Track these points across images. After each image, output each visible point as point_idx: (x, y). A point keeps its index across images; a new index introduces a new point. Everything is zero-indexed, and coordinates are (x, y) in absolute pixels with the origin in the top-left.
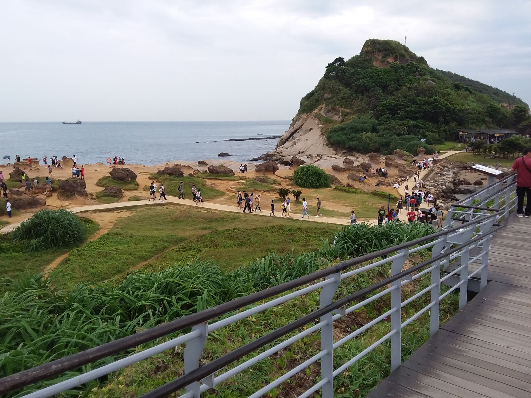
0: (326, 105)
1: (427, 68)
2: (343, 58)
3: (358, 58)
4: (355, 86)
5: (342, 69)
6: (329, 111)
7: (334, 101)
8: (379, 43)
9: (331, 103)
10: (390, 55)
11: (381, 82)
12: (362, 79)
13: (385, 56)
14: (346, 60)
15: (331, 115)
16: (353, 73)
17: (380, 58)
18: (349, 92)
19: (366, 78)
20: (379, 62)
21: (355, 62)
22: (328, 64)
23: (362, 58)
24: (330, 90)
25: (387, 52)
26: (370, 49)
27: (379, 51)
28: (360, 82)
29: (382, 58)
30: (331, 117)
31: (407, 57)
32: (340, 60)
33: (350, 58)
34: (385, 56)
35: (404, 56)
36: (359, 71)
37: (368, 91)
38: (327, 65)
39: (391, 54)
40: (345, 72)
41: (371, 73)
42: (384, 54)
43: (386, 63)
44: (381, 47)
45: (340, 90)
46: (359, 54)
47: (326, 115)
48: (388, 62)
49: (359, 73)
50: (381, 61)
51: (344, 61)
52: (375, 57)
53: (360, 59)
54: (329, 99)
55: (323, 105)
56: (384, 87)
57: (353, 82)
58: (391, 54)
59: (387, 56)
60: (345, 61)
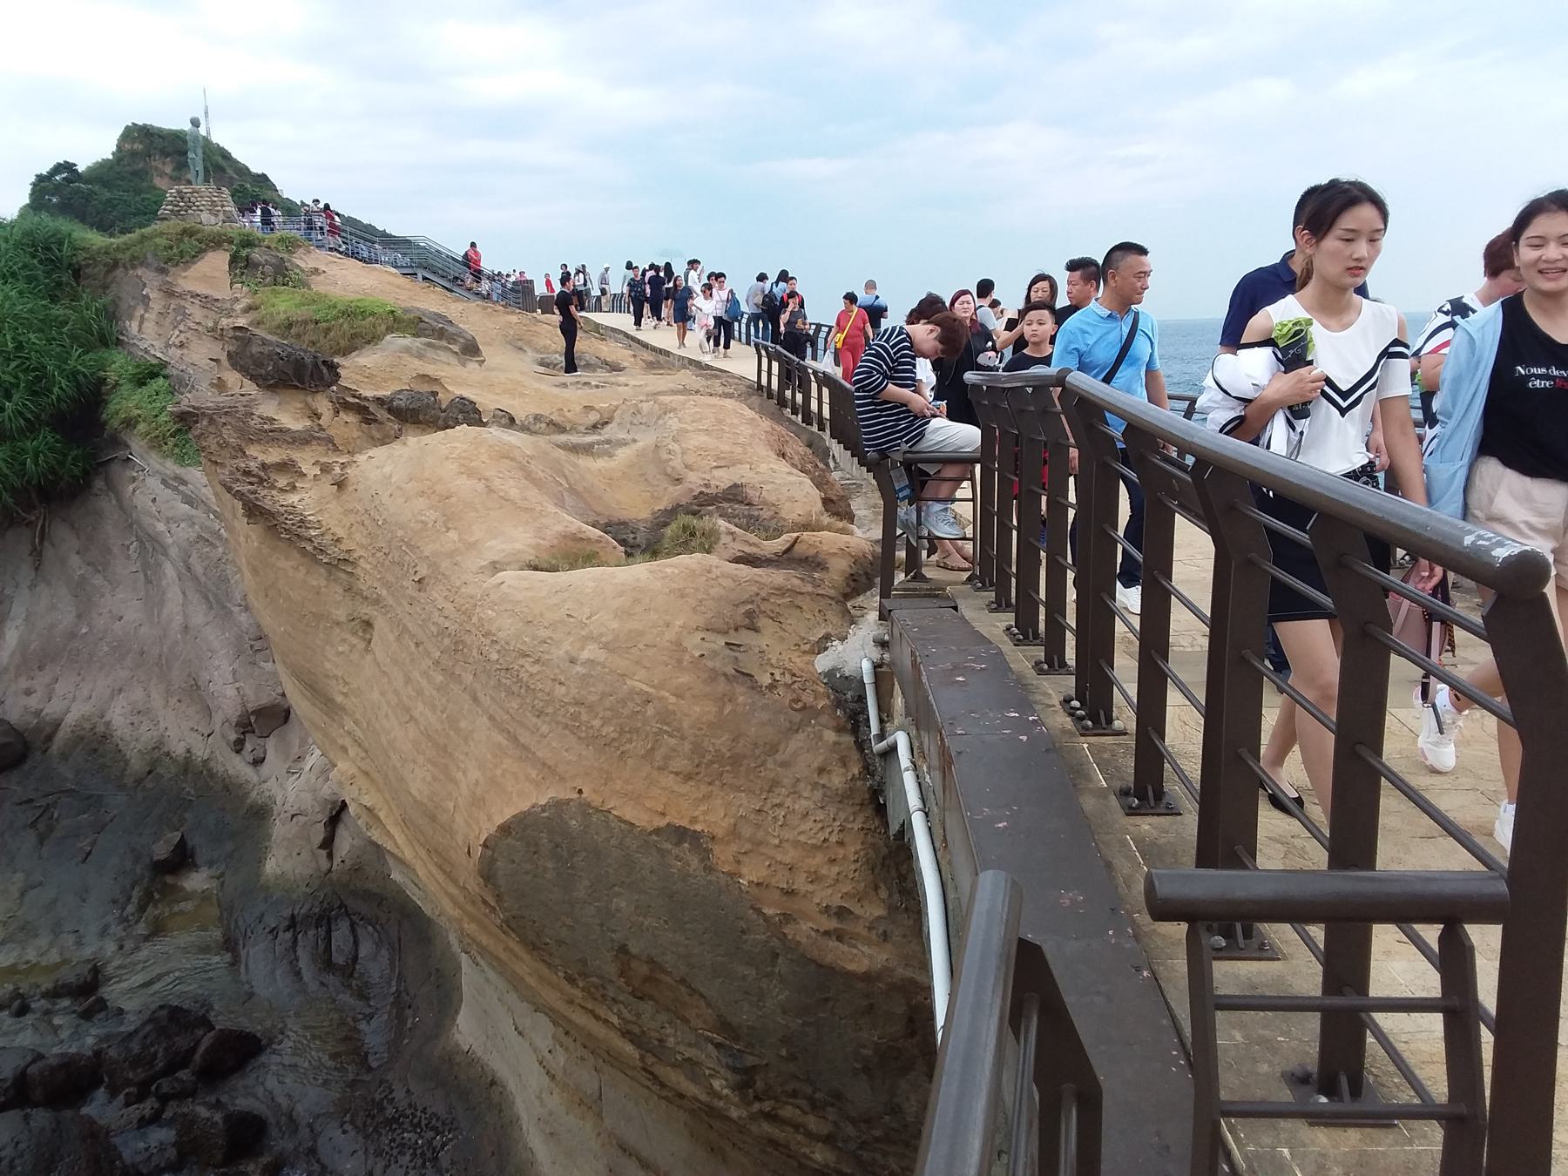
1: (277, 199)
2: (75, 165)
3: (111, 168)
5: (78, 190)
8: (160, 137)
12: (135, 215)
14: (81, 168)
16: (109, 201)
17: (168, 170)
19: (145, 214)
21: (103, 174)
22: (37, 176)
23: (124, 166)
26: (138, 146)
29: (174, 170)
31: (230, 172)
32: (67, 167)
33: (90, 165)
35: (222, 170)
36: (125, 198)
38: (33, 179)
40: (88, 197)
44: (166, 144)
46: (111, 157)
49: (125, 201)
50: (171, 178)
51: (77, 170)
52: (156, 169)
53: (118, 169)
60: (80, 171)
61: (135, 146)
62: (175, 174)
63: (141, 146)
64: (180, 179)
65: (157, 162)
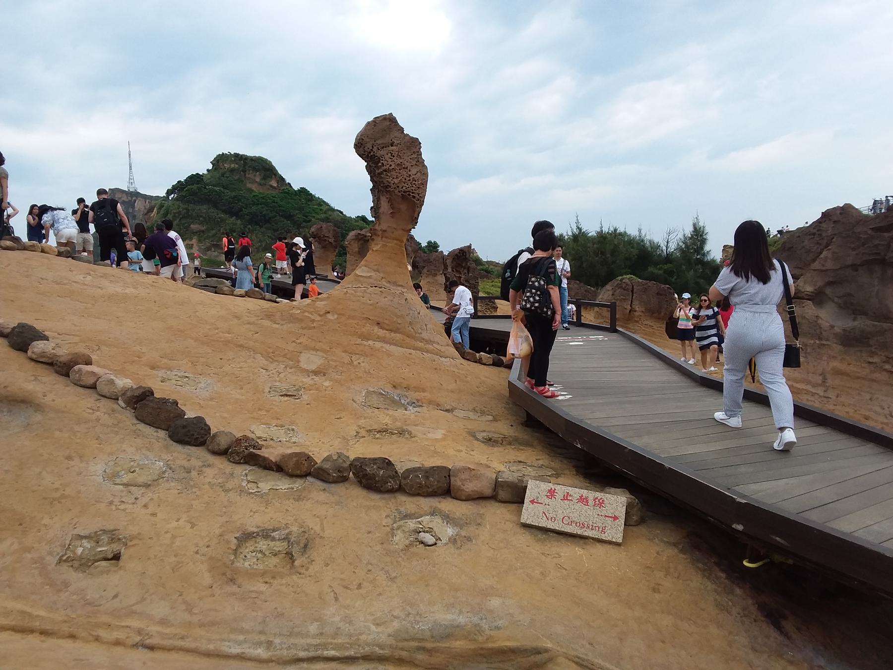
0: (200, 241)
4: (247, 215)
6: (208, 249)
7: (214, 235)
9: (208, 238)
10: (272, 177)
11: (283, 211)
13: (265, 178)
15: (216, 253)
17: (258, 180)
18: (239, 222)
19: (258, 204)
20: (256, 185)
23: (228, 177)
24: (201, 219)
25: (268, 172)
27: (256, 170)
28: (254, 208)
30: (217, 256)
34: (265, 178)
37: (268, 221)
39: (273, 176)
41: (263, 198)
42: (264, 175)
43: (268, 187)
45: (222, 220)
47: (206, 255)
48: (271, 186)
54: (203, 232)
55: (191, 239)
56: (289, 217)
57: (241, 210)
58: (273, 176)
59: (269, 177)
61: (233, 166)
62: (263, 181)
63: (237, 166)
64: (265, 185)
65: (251, 175)
